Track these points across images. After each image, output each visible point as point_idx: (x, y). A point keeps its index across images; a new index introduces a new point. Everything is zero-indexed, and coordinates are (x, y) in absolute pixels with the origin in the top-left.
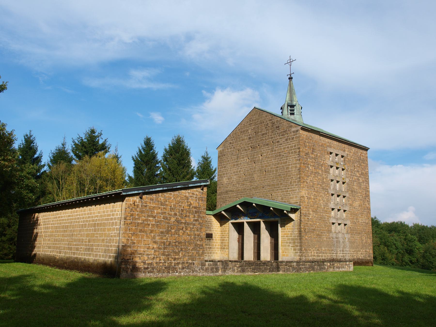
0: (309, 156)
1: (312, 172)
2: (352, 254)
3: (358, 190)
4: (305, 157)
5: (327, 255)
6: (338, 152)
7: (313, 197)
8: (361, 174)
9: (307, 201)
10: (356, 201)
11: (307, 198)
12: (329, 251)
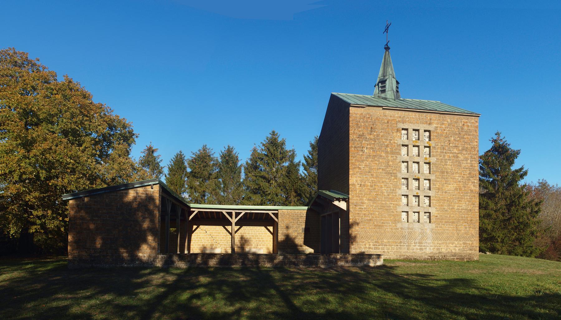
0: (364, 138)
1: (370, 156)
2: (438, 247)
3: (455, 170)
4: (357, 139)
5: (392, 248)
6: (419, 126)
7: (369, 184)
8: (463, 150)
9: (359, 189)
10: (450, 184)
11: (359, 185)
12: (396, 243)
